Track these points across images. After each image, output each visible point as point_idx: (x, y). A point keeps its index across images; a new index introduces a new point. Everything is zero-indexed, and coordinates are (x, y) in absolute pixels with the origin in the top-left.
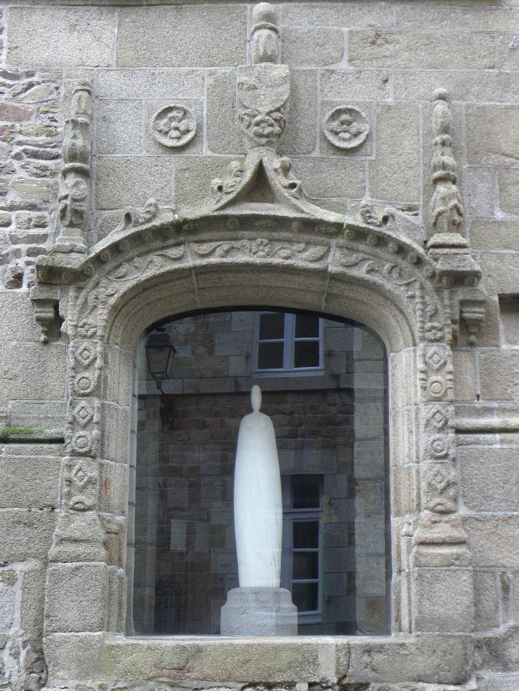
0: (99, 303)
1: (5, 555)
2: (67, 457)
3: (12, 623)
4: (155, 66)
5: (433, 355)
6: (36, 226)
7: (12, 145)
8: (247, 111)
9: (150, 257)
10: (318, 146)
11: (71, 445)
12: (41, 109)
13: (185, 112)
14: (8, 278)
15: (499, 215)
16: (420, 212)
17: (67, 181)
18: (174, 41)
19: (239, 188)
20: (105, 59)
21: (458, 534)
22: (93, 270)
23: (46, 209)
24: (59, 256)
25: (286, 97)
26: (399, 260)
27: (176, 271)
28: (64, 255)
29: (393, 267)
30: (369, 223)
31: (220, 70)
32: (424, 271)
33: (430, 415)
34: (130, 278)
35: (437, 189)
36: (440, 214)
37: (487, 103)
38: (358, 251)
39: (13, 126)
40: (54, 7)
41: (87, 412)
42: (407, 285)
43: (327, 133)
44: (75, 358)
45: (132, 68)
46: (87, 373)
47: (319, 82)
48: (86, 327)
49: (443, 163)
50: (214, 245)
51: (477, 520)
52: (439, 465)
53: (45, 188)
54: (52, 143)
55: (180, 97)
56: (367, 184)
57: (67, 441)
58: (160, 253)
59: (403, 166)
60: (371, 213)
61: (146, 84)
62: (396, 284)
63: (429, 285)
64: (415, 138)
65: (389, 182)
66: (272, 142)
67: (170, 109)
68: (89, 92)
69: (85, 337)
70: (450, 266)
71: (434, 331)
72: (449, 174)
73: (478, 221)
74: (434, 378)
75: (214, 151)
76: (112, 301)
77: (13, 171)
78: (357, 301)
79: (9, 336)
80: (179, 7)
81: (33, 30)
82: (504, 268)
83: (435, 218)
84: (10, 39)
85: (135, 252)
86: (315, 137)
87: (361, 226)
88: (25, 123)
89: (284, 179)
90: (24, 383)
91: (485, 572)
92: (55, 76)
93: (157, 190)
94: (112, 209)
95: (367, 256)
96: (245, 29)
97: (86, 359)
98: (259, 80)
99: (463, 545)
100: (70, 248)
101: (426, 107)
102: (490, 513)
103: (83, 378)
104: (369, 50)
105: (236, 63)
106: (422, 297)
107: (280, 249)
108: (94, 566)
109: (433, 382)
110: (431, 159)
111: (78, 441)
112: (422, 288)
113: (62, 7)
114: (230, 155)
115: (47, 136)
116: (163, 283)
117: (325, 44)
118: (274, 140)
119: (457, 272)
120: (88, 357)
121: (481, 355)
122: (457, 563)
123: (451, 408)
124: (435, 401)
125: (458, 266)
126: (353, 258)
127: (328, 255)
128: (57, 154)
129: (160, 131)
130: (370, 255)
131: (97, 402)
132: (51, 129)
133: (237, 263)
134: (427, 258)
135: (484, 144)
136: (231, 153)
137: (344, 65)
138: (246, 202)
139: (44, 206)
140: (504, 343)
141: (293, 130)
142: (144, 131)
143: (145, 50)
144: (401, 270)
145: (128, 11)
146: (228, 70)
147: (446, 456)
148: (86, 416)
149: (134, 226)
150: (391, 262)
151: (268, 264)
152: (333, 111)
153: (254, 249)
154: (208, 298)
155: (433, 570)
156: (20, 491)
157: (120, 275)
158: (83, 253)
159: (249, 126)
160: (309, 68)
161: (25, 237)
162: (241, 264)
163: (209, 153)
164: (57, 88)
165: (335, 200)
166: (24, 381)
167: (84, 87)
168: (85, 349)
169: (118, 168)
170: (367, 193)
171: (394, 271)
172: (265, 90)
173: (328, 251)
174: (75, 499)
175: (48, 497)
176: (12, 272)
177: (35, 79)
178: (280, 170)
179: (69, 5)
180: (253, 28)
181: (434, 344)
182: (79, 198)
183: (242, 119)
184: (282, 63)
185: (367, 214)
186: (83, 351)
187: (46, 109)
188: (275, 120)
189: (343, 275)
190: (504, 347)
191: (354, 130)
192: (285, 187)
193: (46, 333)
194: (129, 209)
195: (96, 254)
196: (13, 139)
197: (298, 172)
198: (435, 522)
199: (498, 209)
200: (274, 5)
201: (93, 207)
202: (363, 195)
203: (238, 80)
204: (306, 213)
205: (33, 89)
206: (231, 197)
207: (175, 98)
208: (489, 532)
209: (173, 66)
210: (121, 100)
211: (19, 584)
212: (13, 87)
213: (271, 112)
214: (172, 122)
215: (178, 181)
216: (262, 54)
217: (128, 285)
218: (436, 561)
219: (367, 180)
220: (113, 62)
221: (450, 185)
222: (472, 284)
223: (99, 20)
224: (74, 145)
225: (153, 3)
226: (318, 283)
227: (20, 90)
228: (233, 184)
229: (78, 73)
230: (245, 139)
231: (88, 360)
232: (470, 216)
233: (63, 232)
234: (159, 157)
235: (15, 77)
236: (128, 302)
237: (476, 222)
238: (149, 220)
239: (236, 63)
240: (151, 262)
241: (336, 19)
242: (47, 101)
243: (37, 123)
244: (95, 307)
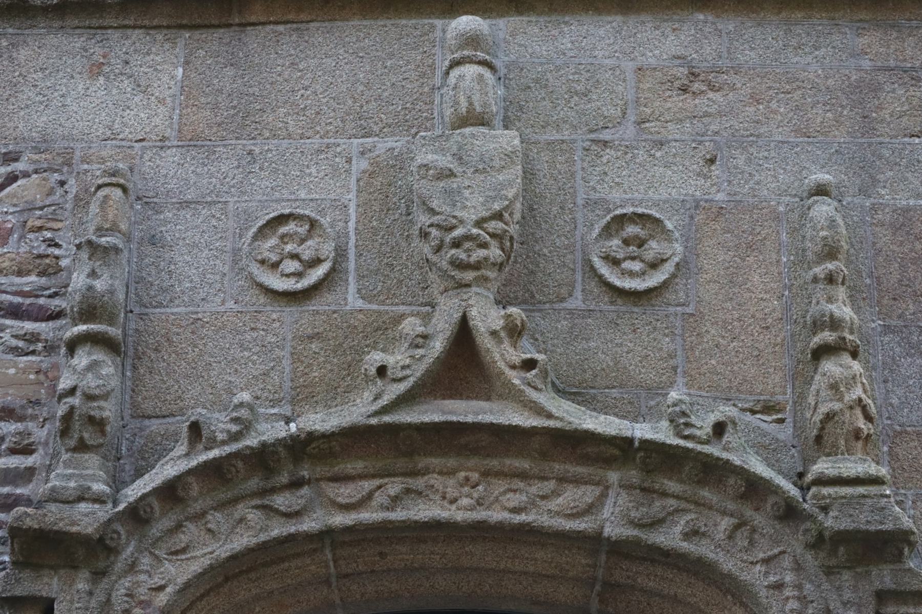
0: (133, 604)
4: (253, 138)
6: (13, 451)
8: (436, 219)
9: (241, 510)
10: (579, 287)
12: (29, 224)
13: (313, 224)
16: (788, 415)
17: (75, 361)
19: (420, 370)
20: (156, 126)
22: (123, 537)
23: (34, 418)
24: (53, 507)
25: (511, 193)
26: (749, 513)
27: (291, 538)
29: (737, 527)
30: (686, 438)
31: (383, 145)
32: (801, 532)
34: (198, 553)
35: (820, 370)
36: (829, 417)
37: (912, 202)
38: (664, 494)
42: (766, 561)
43: (598, 263)
45: (208, 143)
49: (832, 316)
50: (367, 485)
53: (32, 377)
54: (49, 288)
55: (303, 196)
56: (679, 360)
59: (750, 325)
60: (689, 417)
63: (810, 559)
65: (722, 357)
66: (486, 279)
67: (282, 219)
68: (125, 190)
70: (854, 522)
72: (844, 339)
73: (906, 432)
78: (663, 597)
80: (303, 26)
81: (20, 74)
83: (819, 425)
86: (574, 270)
87: (668, 442)
89: (511, 350)
94: (164, 417)
95: (684, 505)
96: (432, 67)
98: (460, 158)
104: (677, 102)
105: (413, 131)
106: (799, 587)
107: (505, 493)
110: (807, 311)
112: (798, 567)
113: (78, 31)
115: (40, 274)
116: (265, 565)
117: (590, 91)
118: (491, 274)
119: (867, 531)
125: (868, 522)
126: (658, 506)
127: (603, 505)
128: (58, 309)
129: (263, 262)
130: (688, 502)
132: (47, 261)
133: (416, 522)
134: (806, 506)
135: (909, 280)
136: (403, 304)
138: (435, 399)
139: (30, 411)
141: (528, 257)
143: (234, 107)
144: (754, 530)
145: (204, 36)
146: (397, 143)
150: (732, 515)
151: (478, 522)
152: (608, 218)
153: (451, 492)
154: (358, 596)
157: (178, 548)
159: (438, 249)
160: (558, 137)
162: (425, 523)
163: (360, 304)
164: (62, 183)
167: (114, 180)
169: (178, 334)
170: (680, 380)
171: (739, 534)
173: (604, 496)
177: (20, 166)
178: (503, 334)
179: (90, 28)
180: (447, 63)
182: (97, 392)
183: (424, 235)
184: (506, 127)
187: (38, 223)
188: (492, 236)
189: (636, 543)
191: (649, 256)
192: (513, 367)
194: (198, 413)
195: (130, 504)
197: (540, 339)
200: (488, 21)
201: (127, 413)
202: (672, 384)
203: (419, 160)
204: (557, 418)
205: (15, 185)
206: (402, 387)
207: (293, 197)
209: (290, 136)
210: (185, 204)
215: (296, 357)
216: (464, 110)
217: (193, 568)
221: (846, 359)
222: (899, 557)
223: (148, 54)
224: (90, 288)
225: (252, 21)
226: (583, 561)
228: (408, 361)
229: (104, 153)
230: (432, 276)
232: (889, 422)
233: (64, 462)
234: (260, 312)
236: (193, 603)
237: (901, 433)
239: (413, 131)
240: (242, 520)
241: (609, 45)
242: (41, 208)
243: (22, 250)
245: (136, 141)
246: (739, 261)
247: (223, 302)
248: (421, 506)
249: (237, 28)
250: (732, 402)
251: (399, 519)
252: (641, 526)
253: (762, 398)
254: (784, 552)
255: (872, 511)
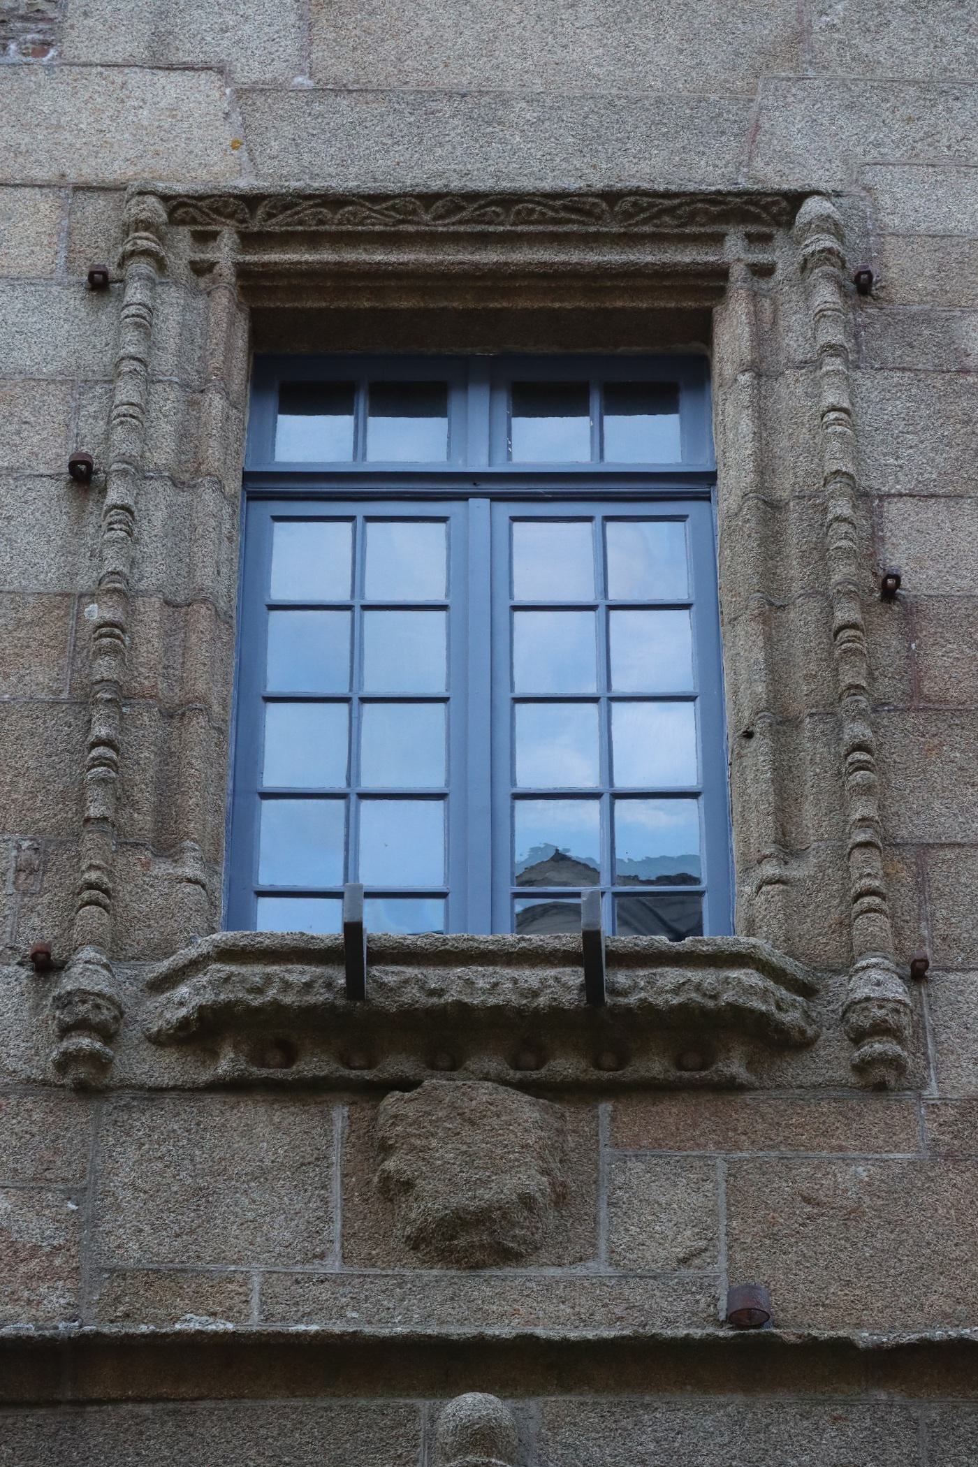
80: (185, 1406)
145: (10, 1421)
225: (95, 1396)
241: (722, 1446)
249: (68, 1409)
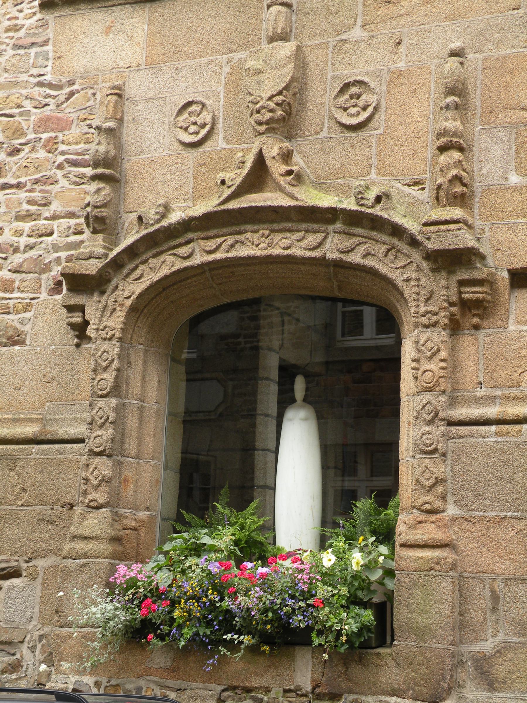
1: (30, 551)
2: (85, 457)
3: (32, 617)
5: (426, 342)
6: (75, 233)
7: (56, 156)
9: (162, 258)
10: (326, 125)
11: (92, 444)
13: (203, 105)
14: (50, 285)
15: (514, 179)
16: (426, 186)
18: (196, 31)
19: (239, 180)
20: (136, 59)
21: (440, 536)
27: (185, 269)
28: (84, 262)
29: (389, 250)
30: (362, 205)
31: (236, 56)
33: (420, 407)
38: (354, 235)
39: (56, 137)
40: (92, 11)
41: (104, 412)
42: (404, 267)
44: (96, 361)
45: (159, 65)
46: (105, 375)
47: (330, 55)
48: (107, 329)
50: (220, 240)
51: (466, 520)
52: (428, 461)
53: (82, 196)
55: (200, 90)
56: (374, 161)
57: (87, 441)
58: (172, 252)
61: (171, 80)
62: (392, 268)
63: (425, 265)
64: (426, 104)
65: (395, 157)
66: (274, 129)
67: (189, 104)
69: (105, 339)
71: (429, 315)
73: (489, 189)
74: (427, 366)
75: (227, 142)
76: (128, 303)
77: (56, 181)
79: (49, 341)
81: (75, 37)
82: (515, 239)
84: (55, 49)
85: (150, 254)
86: (324, 116)
87: (352, 209)
88: (67, 132)
90: (59, 386)
91: (474, 578)
92: (92, 82)
93: (177, 188)
97: (105, 361)
98: (266, 62)
99: (446, 549)
100: (88, 255)
101: (439, 67)
102: (481, 513)
103: (102, 379)
108: (99, 563)
109: (425, 372)
111: (95, 441)
112: (419, 269)
113: (100, 9)
114: (243, 145)
116: (180, 281)
118: (276, 126)
120: (107, 359)
121: (485, 339)
122: (437, 567)
123: (443, 398)
124: (427, 391)
125: (450, 244)
127: (326, 242)
129: (181, 128)
131: (113, 401)
132: (88, 136)
137: (357, 33)
140: (512, 325)
142: (167, 129)
147: (435, 451)
148: (103, 416)
149: (145, 228)
150: (387, 244)
153: (256, 242)
155: (412, 574)
156: (45, 490)
158: (100, 258)
161: (64, 245)
162: (244, 257)
163: (225, 145)
164: (94, 94)
165: (340, 181)
166: (59, 384)
168: (104, 352)
170: (373, 171)
171: (390, 253)
172: (269, 73)
173: (325, 238)
174: (90, 497)
175: (68, 495)
176: (53, 279)
177: (76, 87)
179: (105, 7)
181: (429, 329)
182: (99, 204)
185: (359, 196)
186: (103, 353)
188: (277, 104)
190: (512, 327)
191: (361, 103)
192: (282, 175)
193: (77, 337)
194: (142, 211)
196: (56, 149)
197: (306, 155)
198: (420, 522)
199: (513, 173)
205: (74, 97)
207: (195, 91)
208: (480, 534)
209: (195, 58)
210: (148, 100)
211: (39, 580)
212: (57, 97)
213: (273, 96)
214: (191, 117)
215: (195, 177)
217: (143, 287)
218: (415, 565)
219: (373, 157)
220: (142, 61)
223: (132, 18)
227: (63, 100)
228: (234, 177)
229: (112, 77)
231: (107, 362)
232: (480, 184)
235: (58, 87)
236: (149, 302)
238: (158, 221)
242: (85, 109)
244: (115, 309)
245: (127, 68)
246: (408, 101)
247: (164, 150)
248: (243, 249)
250: (398, 181)
251: (232, 256)
252: (342, 252)
253: (414, 177)
254: (412, 262)
255: (452, 238)
